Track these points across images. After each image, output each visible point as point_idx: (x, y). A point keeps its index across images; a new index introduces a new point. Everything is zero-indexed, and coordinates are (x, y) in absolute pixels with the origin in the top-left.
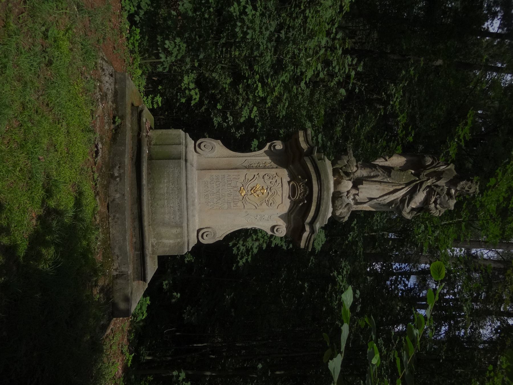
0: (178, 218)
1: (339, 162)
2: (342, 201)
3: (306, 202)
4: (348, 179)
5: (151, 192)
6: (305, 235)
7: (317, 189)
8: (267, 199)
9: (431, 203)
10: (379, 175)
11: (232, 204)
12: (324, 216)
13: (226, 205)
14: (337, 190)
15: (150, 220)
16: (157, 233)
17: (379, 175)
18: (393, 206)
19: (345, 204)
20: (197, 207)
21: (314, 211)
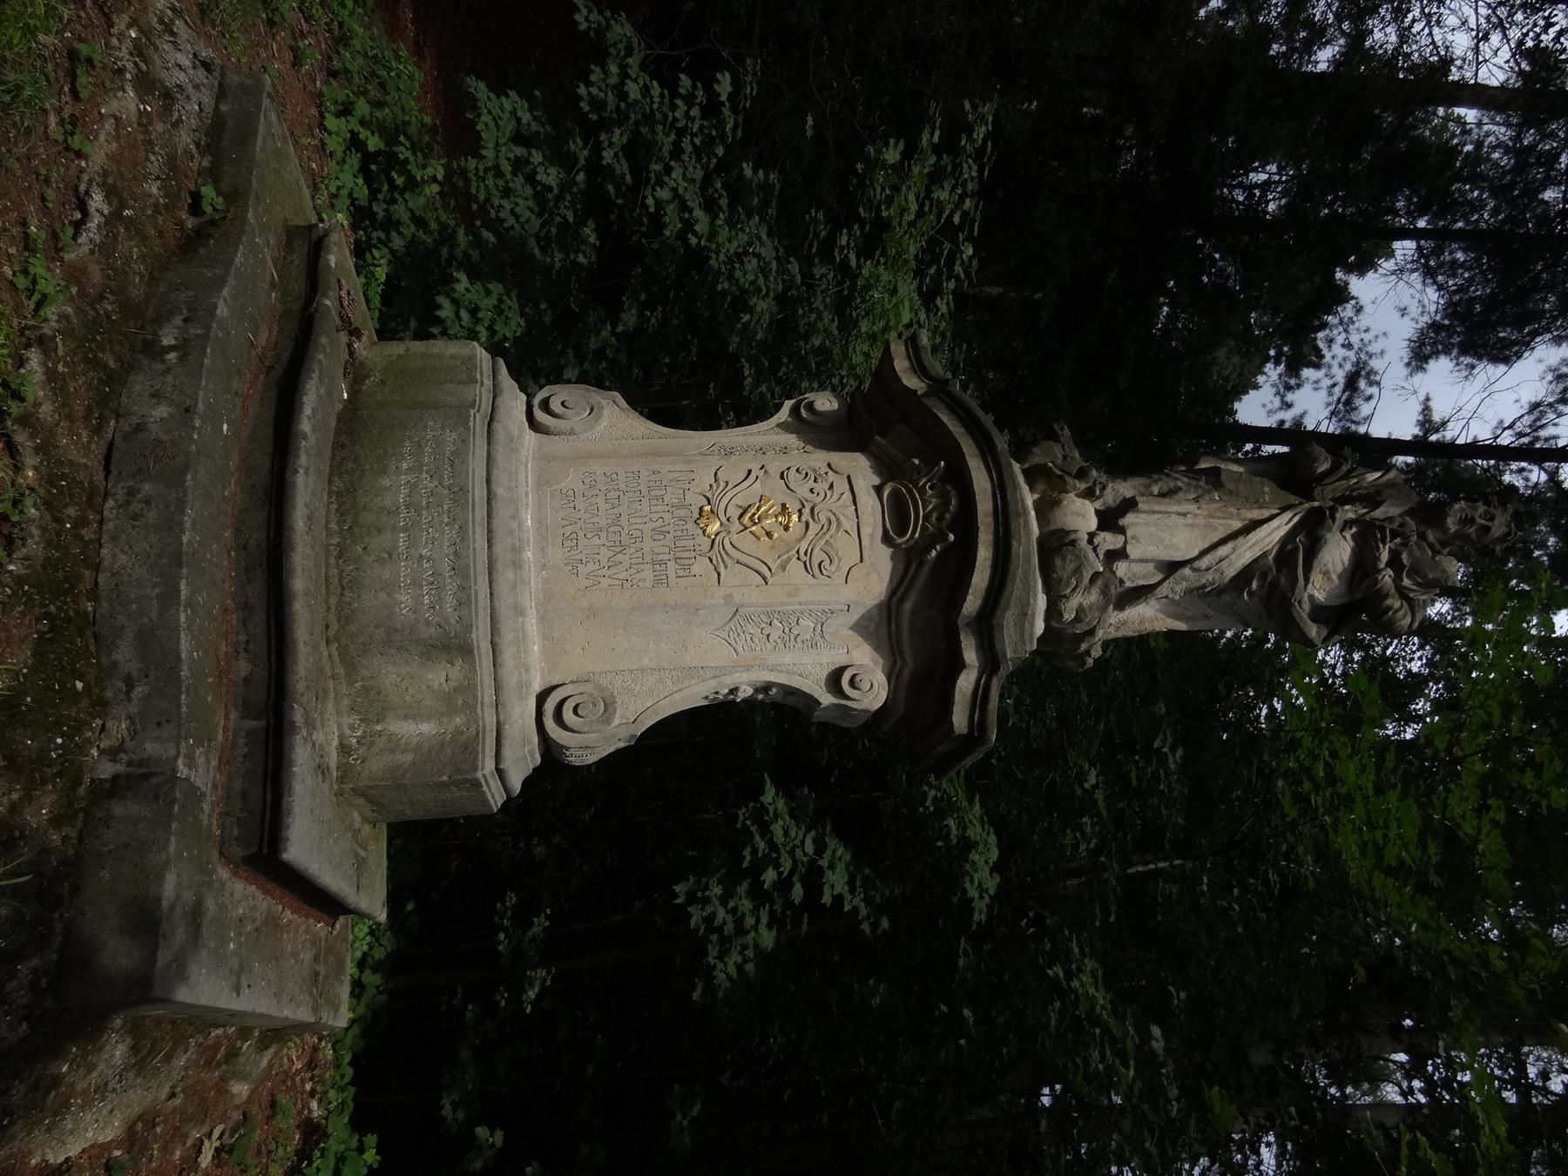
0: (449, 603)
2: (1078, 557)
3: (952, 537)
5: (340, 505)
6: (966, 682)
7: (988, 485)
8: (803, 546)
9: (1382, 565)
10: (1180, 489)
11: (672, 566)
13: (648, 573)
14: (1053, 527)
15: (333, 618)
16: (367, 690)
17: (1180, 489)
18: (1254, 586)
20: (534, 580)
21: (988, 564)
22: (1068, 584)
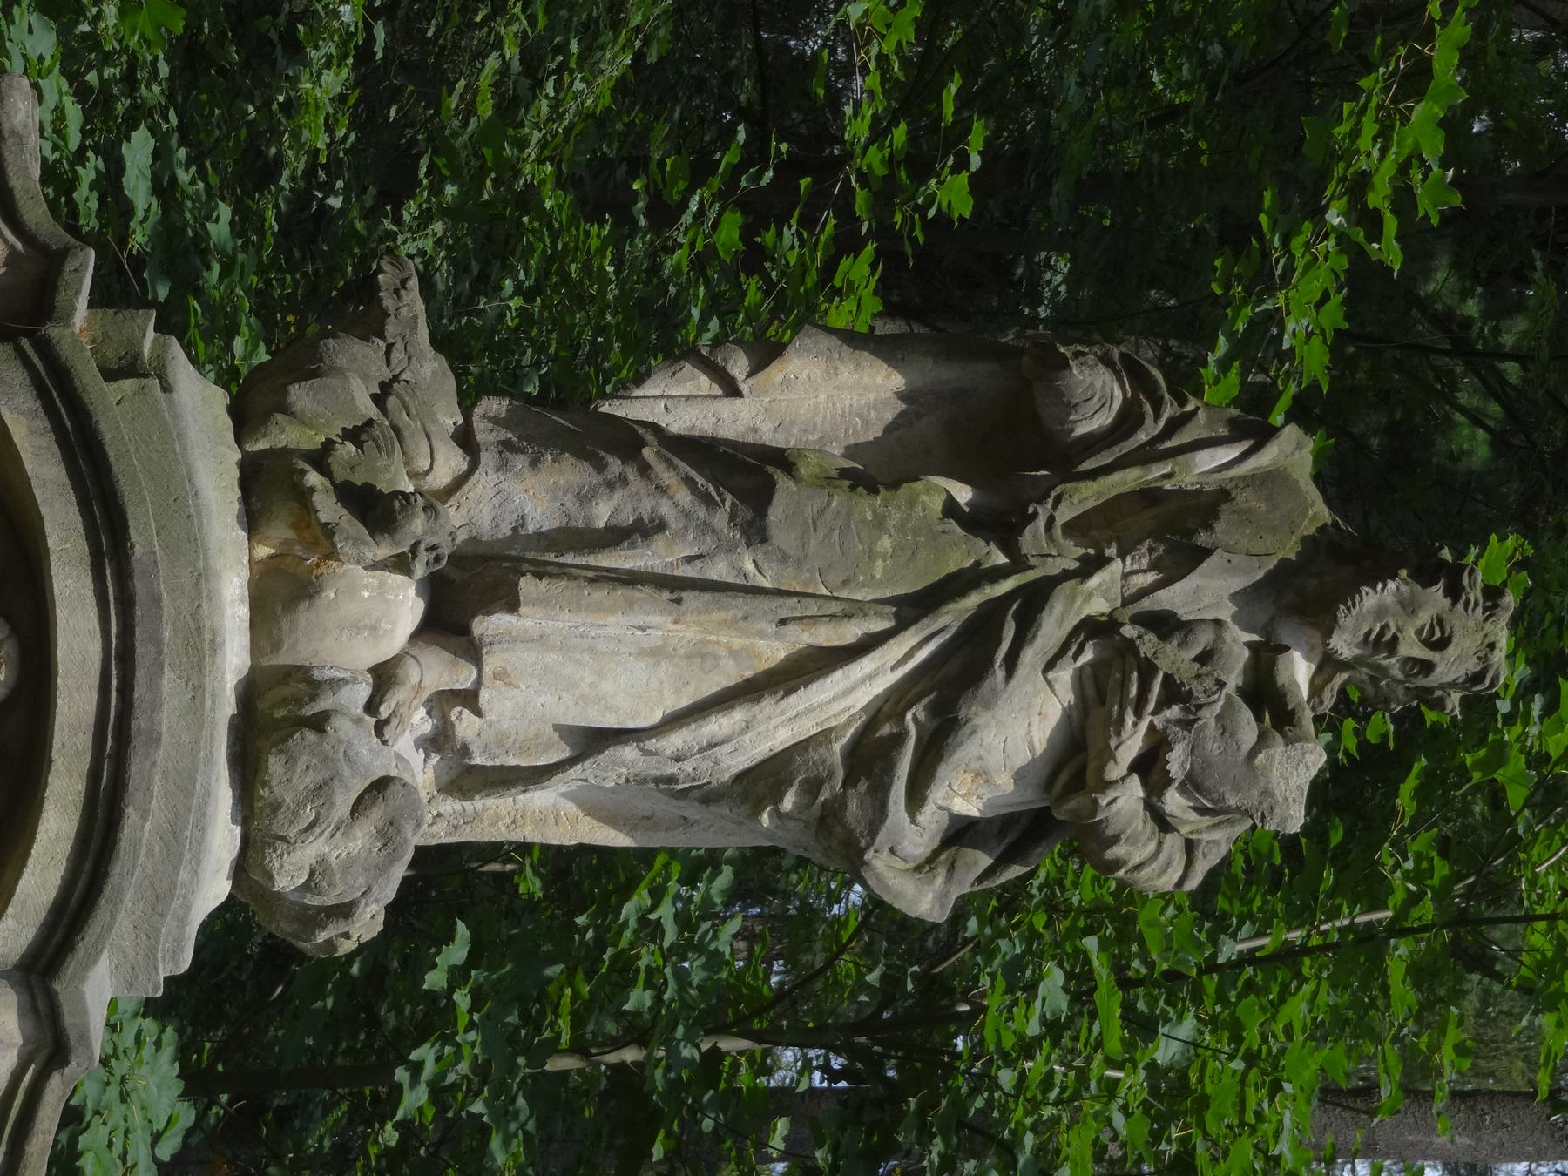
1: (300, 395)
2: (326, 760)
4: (383, 551)
7: (95, 648)
9: (1115, 771)
10: (661, 526)
12: (163, 896)
14: (284, 659)
17: (661, 526)
18: (788, 803)
19: (359, 786)
21: (64, 848)
22: (295, 815)
